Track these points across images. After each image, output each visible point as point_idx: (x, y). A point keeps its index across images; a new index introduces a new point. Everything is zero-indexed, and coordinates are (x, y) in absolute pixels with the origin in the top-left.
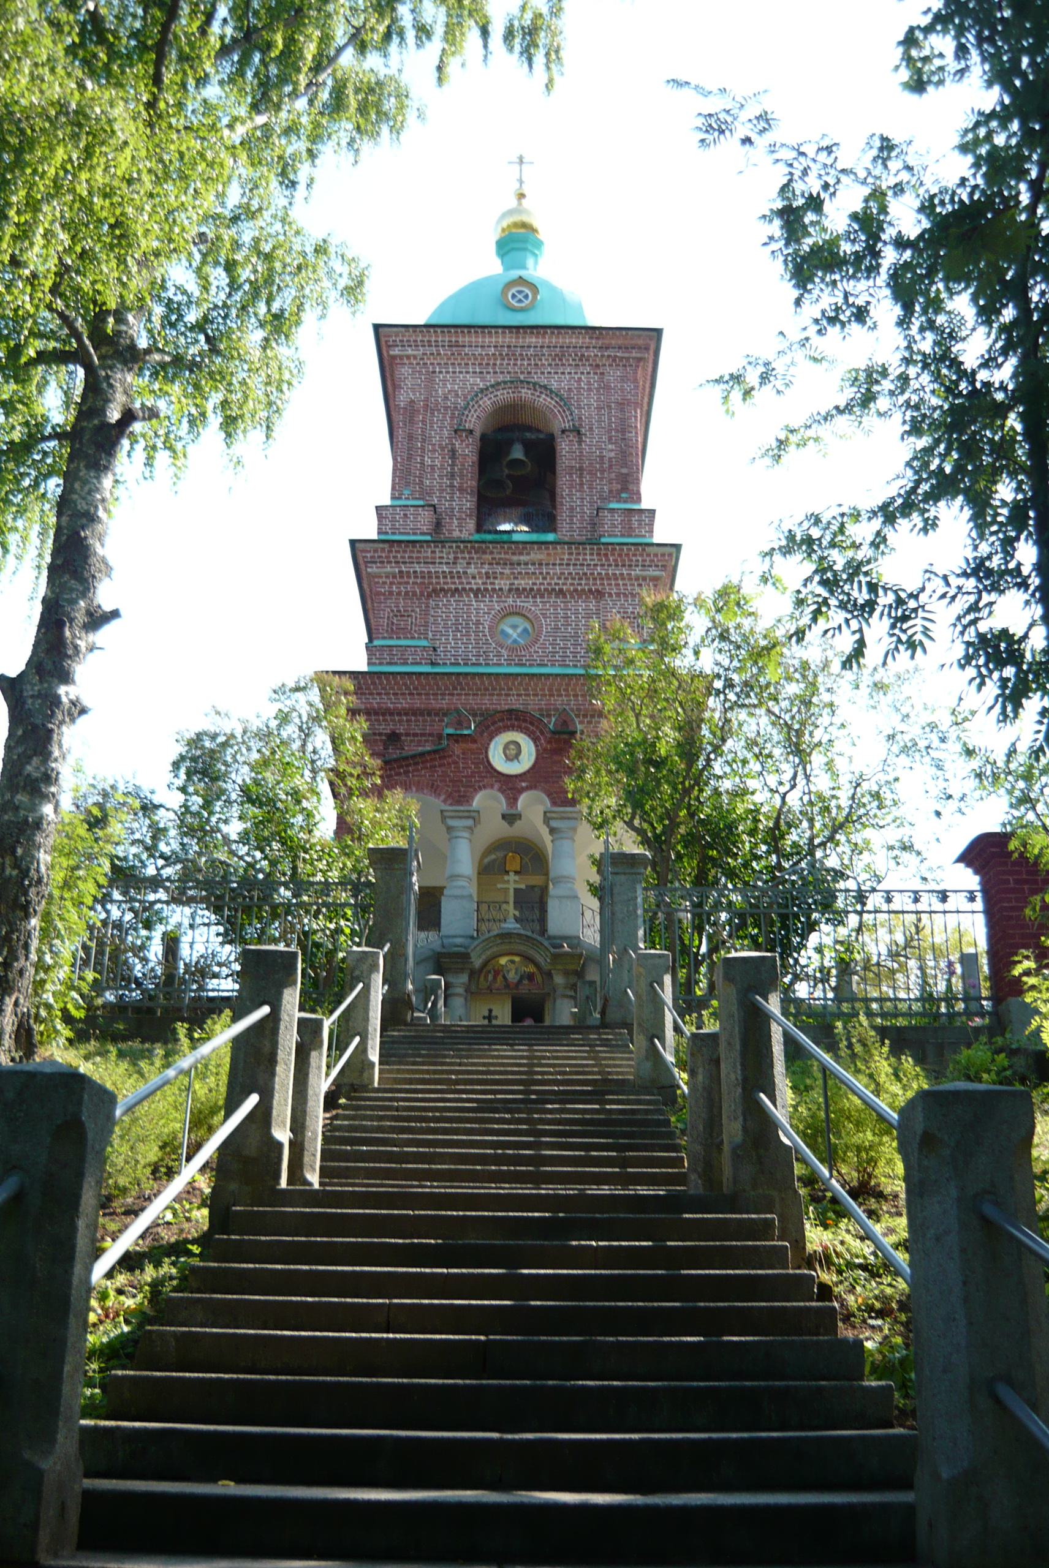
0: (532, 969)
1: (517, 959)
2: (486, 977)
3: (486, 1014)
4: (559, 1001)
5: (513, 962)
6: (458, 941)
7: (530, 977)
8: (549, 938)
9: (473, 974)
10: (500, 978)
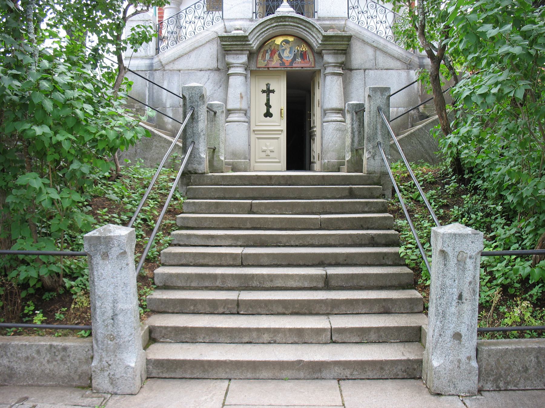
0: (304, 48)
1: (291, 39)
2: (264, 56)
3: (265, 89)
4: (329, 78)
5: (287, 42)
6: (238, 24)
7: (303, 55)
8: (319, 19)
9: (252, 55)
10: (276, 57)
